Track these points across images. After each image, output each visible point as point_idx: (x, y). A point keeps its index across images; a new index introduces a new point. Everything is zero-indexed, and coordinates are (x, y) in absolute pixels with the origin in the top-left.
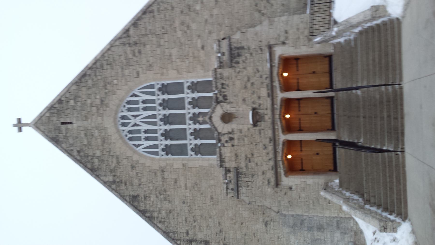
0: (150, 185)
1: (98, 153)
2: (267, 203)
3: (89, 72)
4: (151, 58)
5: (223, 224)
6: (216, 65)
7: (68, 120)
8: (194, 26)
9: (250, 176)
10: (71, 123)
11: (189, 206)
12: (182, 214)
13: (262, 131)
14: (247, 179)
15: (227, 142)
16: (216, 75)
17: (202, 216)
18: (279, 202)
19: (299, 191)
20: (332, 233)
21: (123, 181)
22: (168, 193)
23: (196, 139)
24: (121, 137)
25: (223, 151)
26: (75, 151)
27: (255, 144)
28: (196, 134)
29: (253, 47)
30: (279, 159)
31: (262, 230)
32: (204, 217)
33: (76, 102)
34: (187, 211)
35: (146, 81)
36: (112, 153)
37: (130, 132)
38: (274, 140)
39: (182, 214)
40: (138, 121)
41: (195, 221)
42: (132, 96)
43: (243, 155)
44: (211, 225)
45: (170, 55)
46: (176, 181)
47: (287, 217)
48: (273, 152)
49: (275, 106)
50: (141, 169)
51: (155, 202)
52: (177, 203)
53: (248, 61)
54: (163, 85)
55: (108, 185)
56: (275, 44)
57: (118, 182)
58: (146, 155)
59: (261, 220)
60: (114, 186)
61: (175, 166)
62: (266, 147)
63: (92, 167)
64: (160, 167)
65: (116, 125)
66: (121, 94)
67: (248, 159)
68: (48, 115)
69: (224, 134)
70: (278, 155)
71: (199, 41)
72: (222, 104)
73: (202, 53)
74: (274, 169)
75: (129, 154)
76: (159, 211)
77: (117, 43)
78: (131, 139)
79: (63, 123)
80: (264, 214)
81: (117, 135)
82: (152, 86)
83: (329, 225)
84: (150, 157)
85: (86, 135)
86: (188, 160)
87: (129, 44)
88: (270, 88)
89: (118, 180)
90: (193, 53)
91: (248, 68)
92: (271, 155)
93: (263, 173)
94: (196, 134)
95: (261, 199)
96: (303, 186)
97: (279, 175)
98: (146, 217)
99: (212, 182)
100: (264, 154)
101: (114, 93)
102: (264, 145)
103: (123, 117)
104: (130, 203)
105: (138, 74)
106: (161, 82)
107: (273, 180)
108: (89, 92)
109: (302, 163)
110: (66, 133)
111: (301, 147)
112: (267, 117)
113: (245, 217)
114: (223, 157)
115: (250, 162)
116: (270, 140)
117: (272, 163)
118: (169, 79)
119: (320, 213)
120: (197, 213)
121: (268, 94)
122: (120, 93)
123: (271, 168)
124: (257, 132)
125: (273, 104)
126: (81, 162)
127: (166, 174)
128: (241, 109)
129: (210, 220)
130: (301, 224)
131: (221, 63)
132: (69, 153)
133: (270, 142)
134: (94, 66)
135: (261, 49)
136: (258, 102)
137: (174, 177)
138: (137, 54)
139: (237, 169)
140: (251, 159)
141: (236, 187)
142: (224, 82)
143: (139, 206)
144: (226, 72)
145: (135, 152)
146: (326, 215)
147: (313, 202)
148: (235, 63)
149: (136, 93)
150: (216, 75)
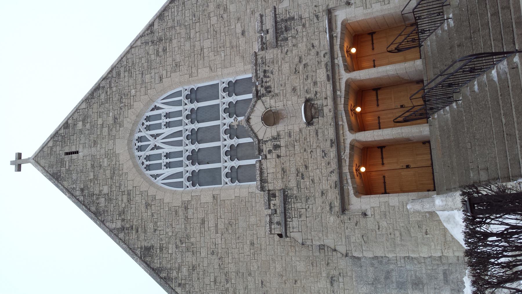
0: (168, 230)
1: (106, 190)
2: (329, 242)
3: (103, 84)
4: (178, 56)
5: (268, 284)
6: (256, 47)
7: (74, 150)
8: (232, 8)
9: (303, 200)
10: (77, 152)
11: (219, 259)
12: (209, 272)
13: (320, 131)
14: (299, 205)
15: (270, 152)
16: (256, 60)
17: (237, 273)
18: (348, 237)
19: (378, 217)
20: (437, 290)
21: (134, 226)
22: (193, 240)
23: (232, 159)
24: (135, 166)
25: (264, 166)
26: (77, 189)
27: (309, 151)
28: (234, 153)
29: (306, 15)
30: (346, 169)
31: (326, 290)
32: (240, 274)
33: (84, 125)
34: (216, 267)
35: (170, 87)
36: (122, 187)
37: (148, 158)
38: (337, 142)
39: (209, 272)
40: (158, 142)
41: (227, 282)
42: (153, 110)
43: (293, 170)
44: (251, 286)
45: (202, 49)
46: (203, 222)
47: (364, 268)
48: (336, 160)
49: (338, 93)
50: (159, 208)
51: (174, 254)
52: (203, 255)
53: (300, 34)
54: (192, 90)
55: (114, 233)
56: (336, 7)
57: (127, 229)
58: (164, 188)
59: (324, 275)
60: (121, 235)
61: (203, 200)
62: (325, 154)
63: (97, 209)
64: (183, 202)
65: (130, 149)
66: (139, 107)
67: (300, 175)
68: (50, 144)
69: (266, 141)
70: (343, 164)
71: (239, 25)
72: (263, 99)
73: (242, 40)
74: (339, 186)
75: (144, 187)
76: (179, 269)
77: (139, 43)
78: (148, 168)
79: (69, 159)
80: (328, 264)
81: (130, 163)
82: (179, 94)
83: (431, 277)
84: (171, 190)
85: (93, 166)
86: (220, 189)
87: (153, 42)
88: (329, 68)
89: (128, 226)
90: (231, 43)
91: (300, 45)
92: (334, 166)
93: (323, 193)
94: (234, 153)
95: (321, 235)
96: (383, 209)
97: (346, 194)
98: (161, 278)
99: (253, 220)
100: (323, 164)
101: (130, 107)
102: (323, 151)
103: (140, 139)
104: (141, 258)
105: (161, 79)
106: (189, 87)
107: (337, 204)
108: (101, 109)
109: (385, 183)
110: (70, 166)
111: (382, 158)
112: (326, 110)
113: (299, 272)
114: (265, 175)
115: (303, 178)
116: (332, 142)
117: (335, 177)
118: (199, 81)
119: (413, 251)
120: (232, 268)
121: (328, 75)
122: (138, 106)
123: (333, 185)
124: (313, 133)
125: (334, 90)
126: (84, 205)
127: (190, 212)
128: (290, 103)
129: (249, 278)
130: (387, 278)
131: (263, 43)
132: (70, 193)
133: (332, 146)
134: (110, 75)
135: (317, 17)
136: (313, 90)
137: (201, 216)
138: (161, 53)
139: (284, 191)
140: (304, 173)
141: (283, 219)
142: (267, 68)
143: (153, 262)
144: (270, 54)
145: (152, 184)
146: (422, 255)
147: (401, 234)
148: (282, 40)
149: (158, 105)
150: (256, 60)
